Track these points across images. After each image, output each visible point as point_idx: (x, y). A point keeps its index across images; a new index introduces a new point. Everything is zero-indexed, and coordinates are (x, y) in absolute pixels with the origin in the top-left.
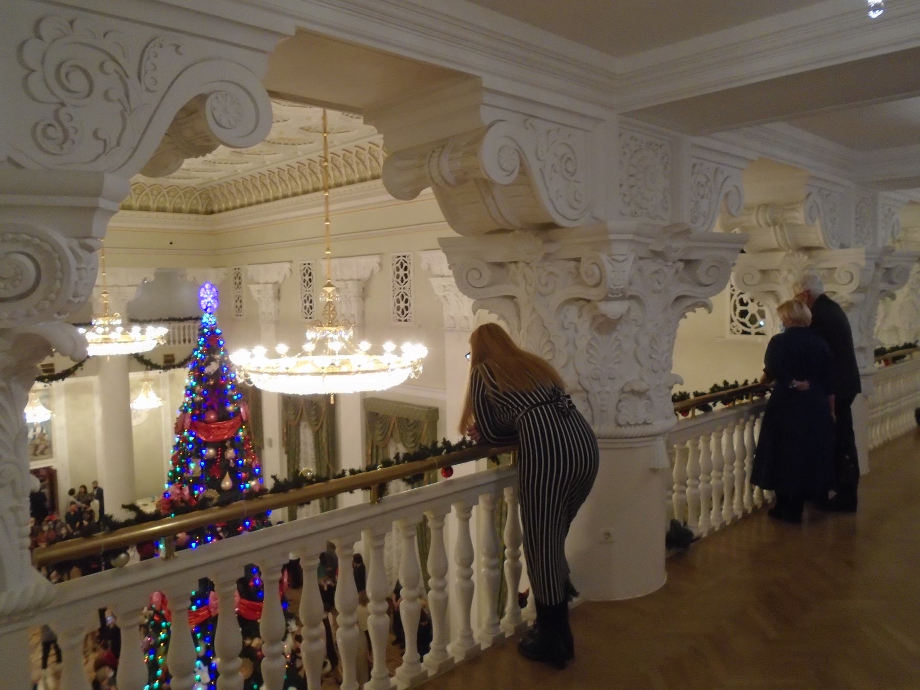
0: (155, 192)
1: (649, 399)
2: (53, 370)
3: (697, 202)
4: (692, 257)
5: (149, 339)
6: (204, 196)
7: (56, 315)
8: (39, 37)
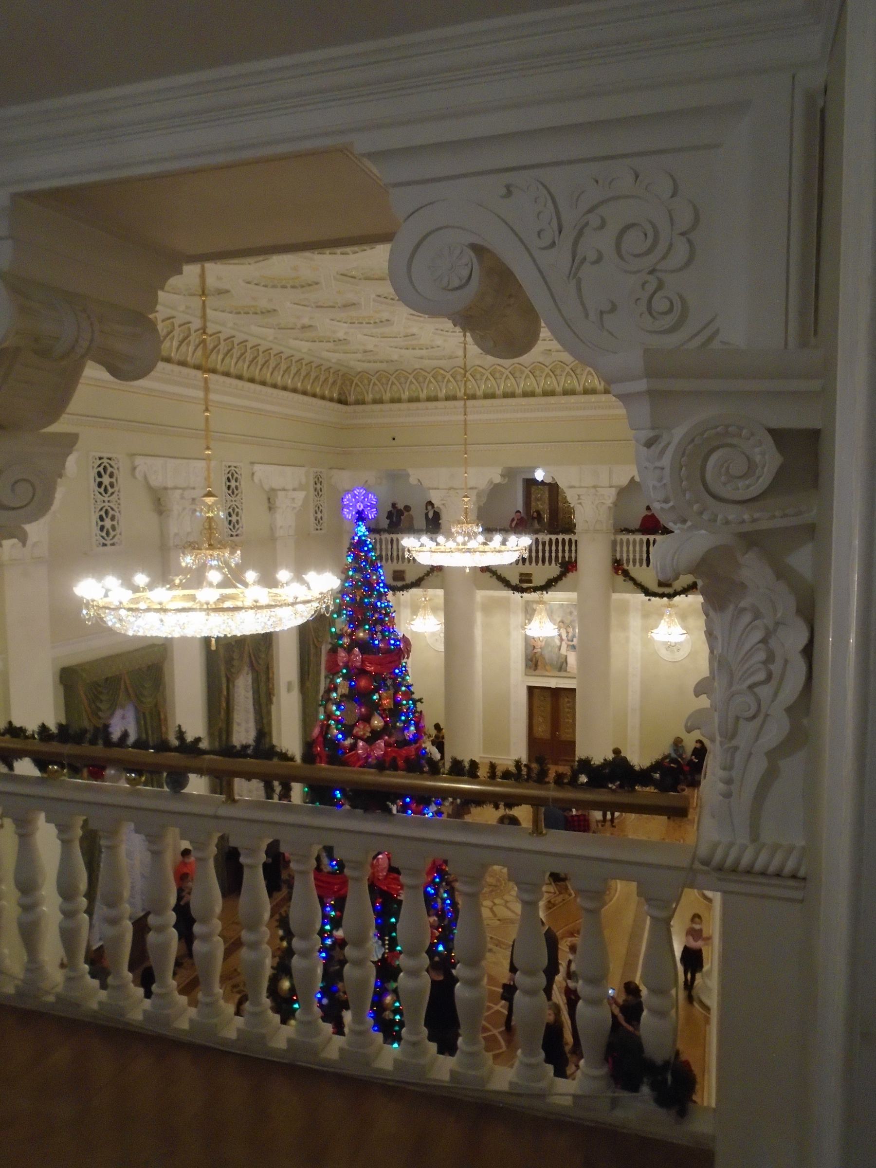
2: (530, 581)
5: (510, 550)
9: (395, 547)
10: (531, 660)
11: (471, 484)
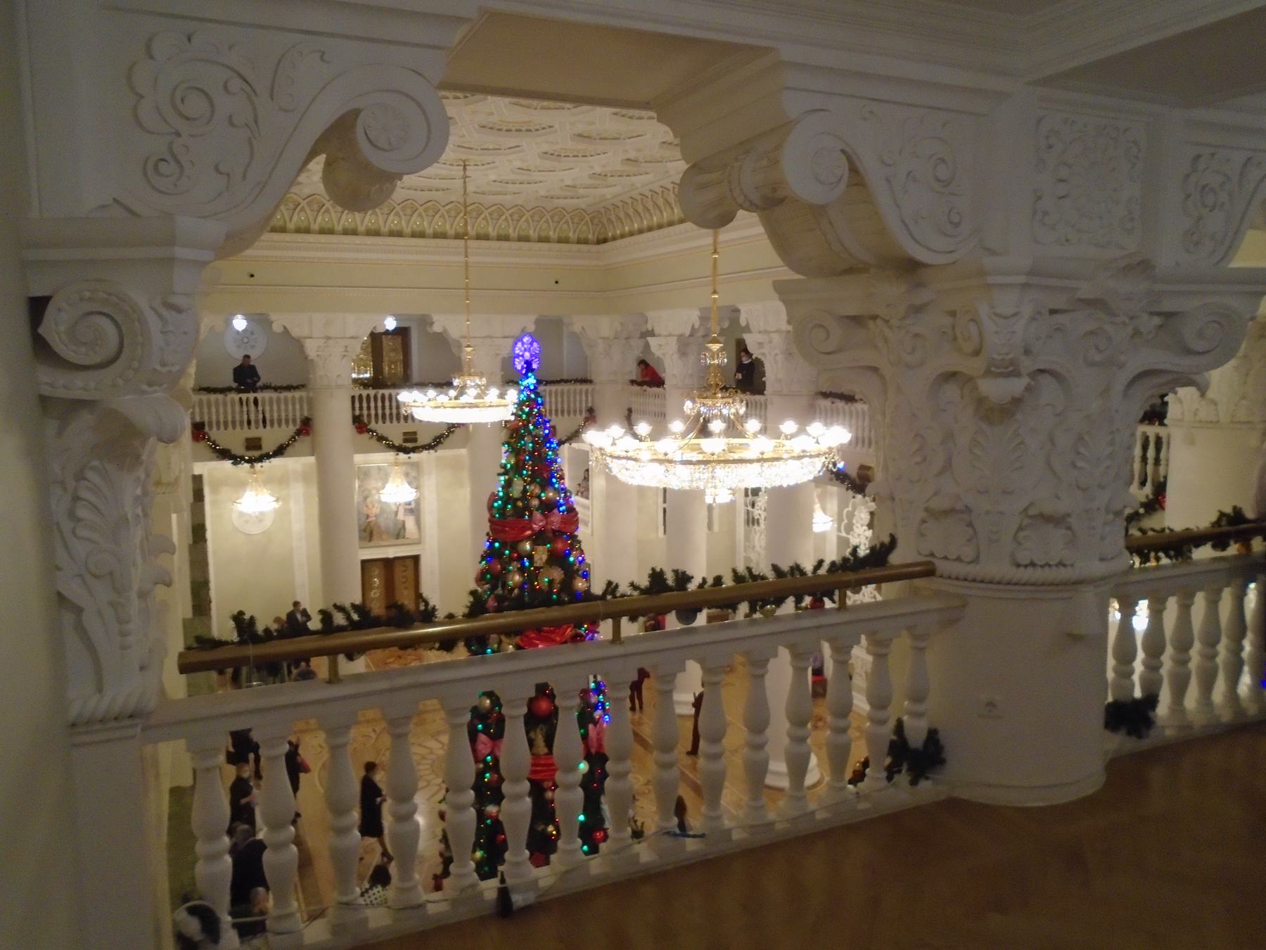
0: (536, 218)
1: (1069, 528)
2: (415, 440)
3: (1200, 218)
4: (1168, 306)
6: (596, 221)
7: (145, 387)
8: (151, 57)
9: (387, 403)
10: (365, 530)
11: (351, 332)
